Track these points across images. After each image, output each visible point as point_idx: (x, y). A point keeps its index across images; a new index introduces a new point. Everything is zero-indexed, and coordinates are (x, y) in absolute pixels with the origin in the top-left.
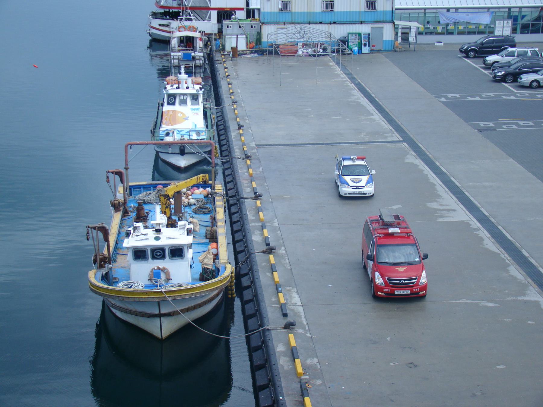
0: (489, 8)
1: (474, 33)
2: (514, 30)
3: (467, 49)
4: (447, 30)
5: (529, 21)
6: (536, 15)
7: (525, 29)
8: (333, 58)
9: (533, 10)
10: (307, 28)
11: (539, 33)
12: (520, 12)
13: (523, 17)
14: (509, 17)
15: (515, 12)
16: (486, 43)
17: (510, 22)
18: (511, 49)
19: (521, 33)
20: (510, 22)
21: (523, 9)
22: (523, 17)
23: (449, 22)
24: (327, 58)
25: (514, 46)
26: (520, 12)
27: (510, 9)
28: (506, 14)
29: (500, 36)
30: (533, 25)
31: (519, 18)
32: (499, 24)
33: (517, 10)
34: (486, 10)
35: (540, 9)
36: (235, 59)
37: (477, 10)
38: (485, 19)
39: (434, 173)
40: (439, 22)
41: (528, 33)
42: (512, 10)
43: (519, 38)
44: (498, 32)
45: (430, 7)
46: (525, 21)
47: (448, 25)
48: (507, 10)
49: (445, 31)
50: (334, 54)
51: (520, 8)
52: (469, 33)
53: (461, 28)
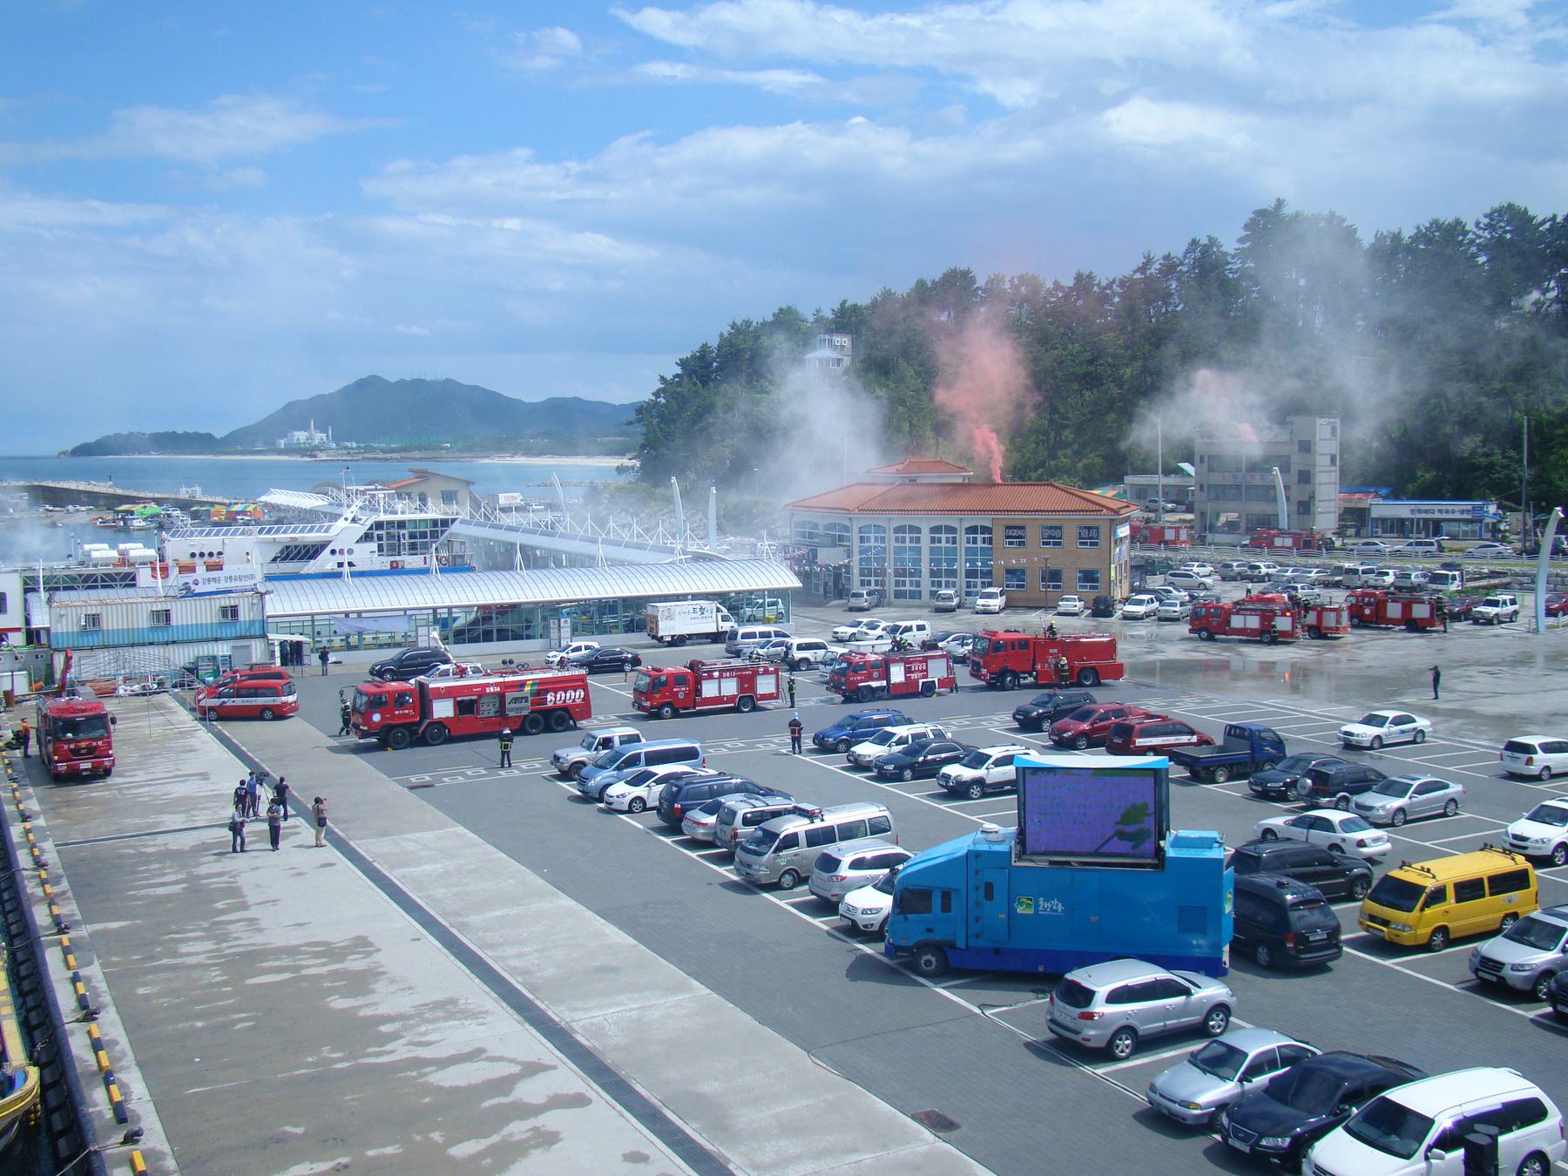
0: (405, 610)
1: (389, 645)
2: (445, 639)
3: (380, 669)
4: (348, 643)
5: (464, 625)
6: (472, 617)
7: (461, 636)
8: (175, 696)
9: (468, 610)
10: (128, 653)
11: (479, 642)
12: (450, 613)
13: (455, 619)
14: (436, 621)
15: (443, 614)
16: (407, 659)
17: (438, 627)
18: (443, 667)
19: (455, 643)
20: (438, 627)
21: (454, 610)
22: (455, 619)
23: (346, 630)
24: (165, 697)
25: (447, 661)
26: (450, 613)
27: (435, 609)
28: (431, 617)
29: (425, 649)
30: (469, 630)
31: (450, 621)
32: (422, 631)
33: (446, 610)
34: (402, 613)
35: (476, 609)
36: (11, 709)
37: (389, 614)
38: (401, 628)
39: (349, 860)
40: (335, 632)
41: (464, 642)
42: (439, 611)
43: (453, 651)
44: (423, 643)
45: (319, 611)
46: (457, 624)
47: (348, 637)
48: (431, 611)
49: (344, 644)
50: (176, 690)
51: (450, 608)
52: (381, 646)
53: (368, 638)
